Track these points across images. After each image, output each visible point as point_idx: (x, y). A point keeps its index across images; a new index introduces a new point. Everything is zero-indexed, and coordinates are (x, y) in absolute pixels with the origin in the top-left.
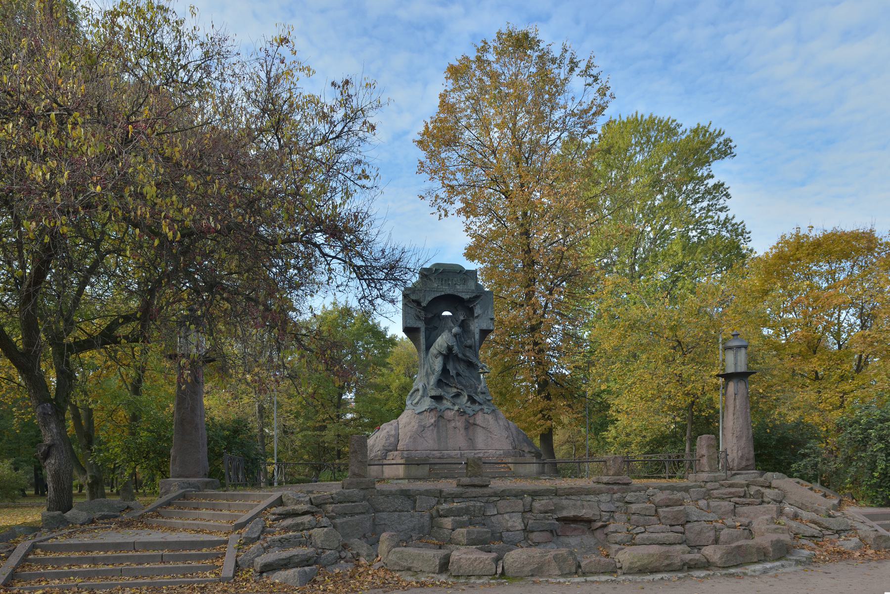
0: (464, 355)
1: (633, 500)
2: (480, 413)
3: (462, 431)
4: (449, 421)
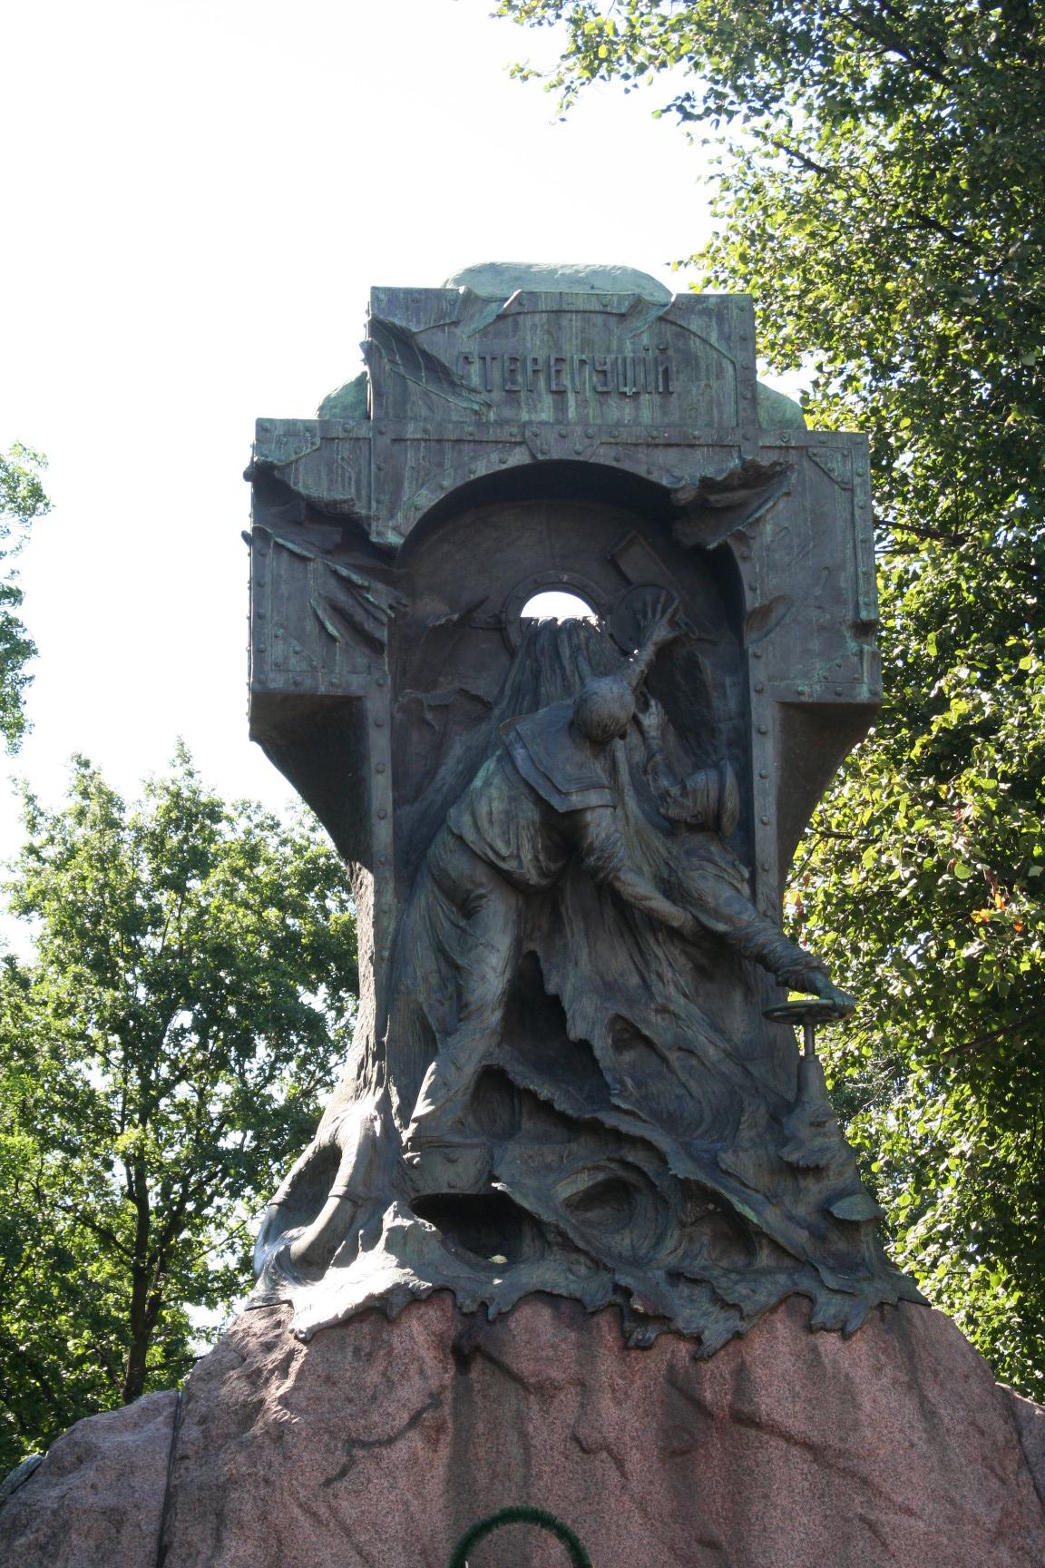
4: (544, 1391)
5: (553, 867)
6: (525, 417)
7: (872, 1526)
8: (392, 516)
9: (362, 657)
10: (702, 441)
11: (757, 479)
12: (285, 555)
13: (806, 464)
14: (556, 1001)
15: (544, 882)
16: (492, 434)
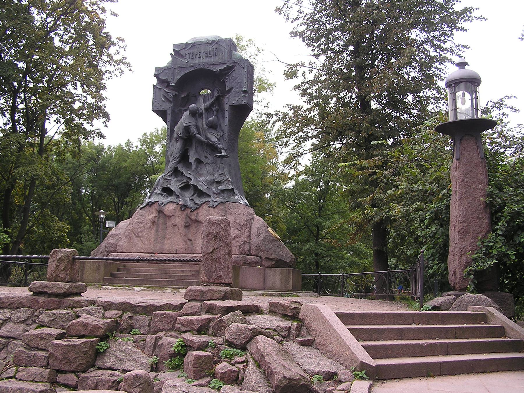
0: (207, 138)
1: (46, 320)
2: (205, 207)
3: (182, 229)
4: (169, 217)
9: (168, 104)
11: (230, 69)
12: (158, 89)
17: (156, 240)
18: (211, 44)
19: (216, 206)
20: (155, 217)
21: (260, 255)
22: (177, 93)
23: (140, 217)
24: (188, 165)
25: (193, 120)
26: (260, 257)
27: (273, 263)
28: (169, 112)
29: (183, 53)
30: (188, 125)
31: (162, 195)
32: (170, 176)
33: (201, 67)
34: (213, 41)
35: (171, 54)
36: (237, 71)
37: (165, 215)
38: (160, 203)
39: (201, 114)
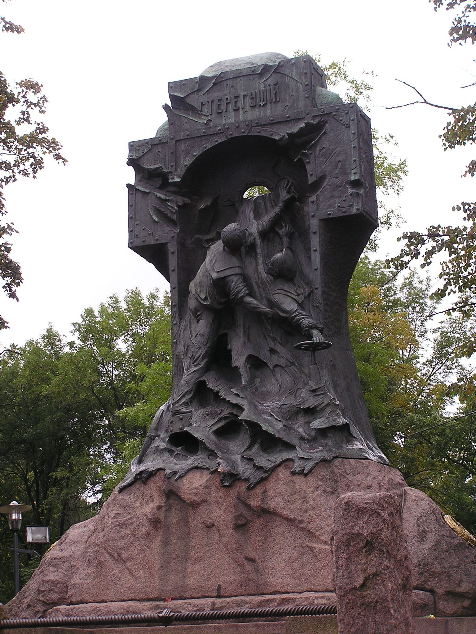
0: (272, 304)
2: (283, 474)
3: (229, 533)
4: (194, 505)
5: (223, 300)
6: (224, 122)
7: (311, 549)
8: (176, 170)
9: (167, 228)
10: (290, 119)
13: (331, 119)
14: (230, 351)
15: (220, 307)
16: (211, 132)
17: (165, 565)
18: (261, 74)
19: (310, 471)
20: (159, 508)
21: (430, 585)
22: (187, 200)
23: (120, 510)
24: (230, 374)
25: (235, 262)
26: (432, 591)
27: (467, 603)
28: (172, 248)
29: (194, 101)
30: (222, 275)
31: (171, 452)
32: (186, 404)
33: (243, 131)
34: (266, 68)
35: (166, 107)
36: (332, 135)
37: (184, 501)
38: (168, 472)
39: (252, 248)
